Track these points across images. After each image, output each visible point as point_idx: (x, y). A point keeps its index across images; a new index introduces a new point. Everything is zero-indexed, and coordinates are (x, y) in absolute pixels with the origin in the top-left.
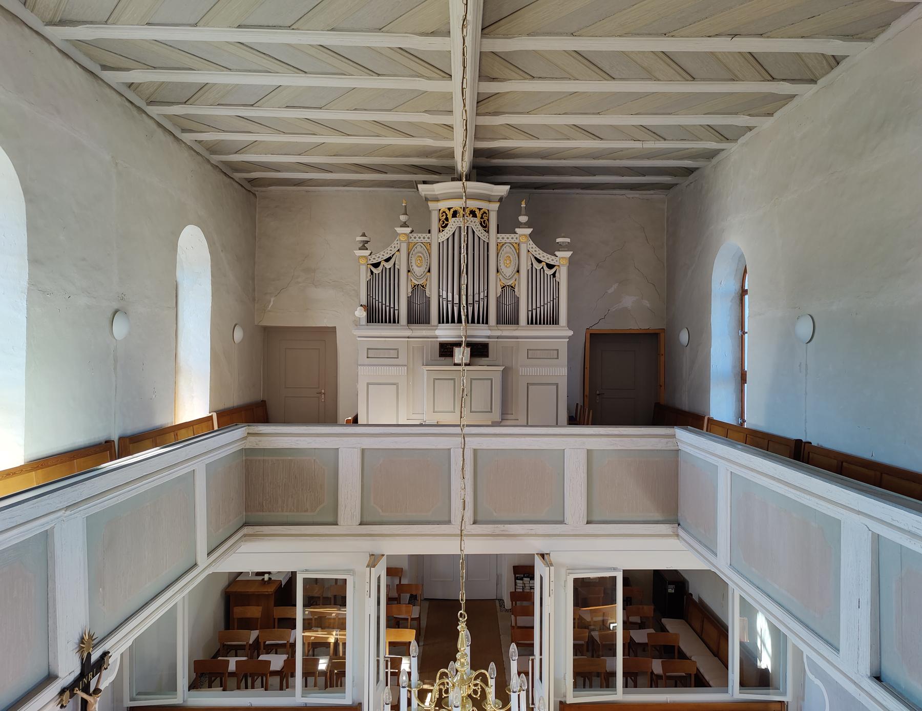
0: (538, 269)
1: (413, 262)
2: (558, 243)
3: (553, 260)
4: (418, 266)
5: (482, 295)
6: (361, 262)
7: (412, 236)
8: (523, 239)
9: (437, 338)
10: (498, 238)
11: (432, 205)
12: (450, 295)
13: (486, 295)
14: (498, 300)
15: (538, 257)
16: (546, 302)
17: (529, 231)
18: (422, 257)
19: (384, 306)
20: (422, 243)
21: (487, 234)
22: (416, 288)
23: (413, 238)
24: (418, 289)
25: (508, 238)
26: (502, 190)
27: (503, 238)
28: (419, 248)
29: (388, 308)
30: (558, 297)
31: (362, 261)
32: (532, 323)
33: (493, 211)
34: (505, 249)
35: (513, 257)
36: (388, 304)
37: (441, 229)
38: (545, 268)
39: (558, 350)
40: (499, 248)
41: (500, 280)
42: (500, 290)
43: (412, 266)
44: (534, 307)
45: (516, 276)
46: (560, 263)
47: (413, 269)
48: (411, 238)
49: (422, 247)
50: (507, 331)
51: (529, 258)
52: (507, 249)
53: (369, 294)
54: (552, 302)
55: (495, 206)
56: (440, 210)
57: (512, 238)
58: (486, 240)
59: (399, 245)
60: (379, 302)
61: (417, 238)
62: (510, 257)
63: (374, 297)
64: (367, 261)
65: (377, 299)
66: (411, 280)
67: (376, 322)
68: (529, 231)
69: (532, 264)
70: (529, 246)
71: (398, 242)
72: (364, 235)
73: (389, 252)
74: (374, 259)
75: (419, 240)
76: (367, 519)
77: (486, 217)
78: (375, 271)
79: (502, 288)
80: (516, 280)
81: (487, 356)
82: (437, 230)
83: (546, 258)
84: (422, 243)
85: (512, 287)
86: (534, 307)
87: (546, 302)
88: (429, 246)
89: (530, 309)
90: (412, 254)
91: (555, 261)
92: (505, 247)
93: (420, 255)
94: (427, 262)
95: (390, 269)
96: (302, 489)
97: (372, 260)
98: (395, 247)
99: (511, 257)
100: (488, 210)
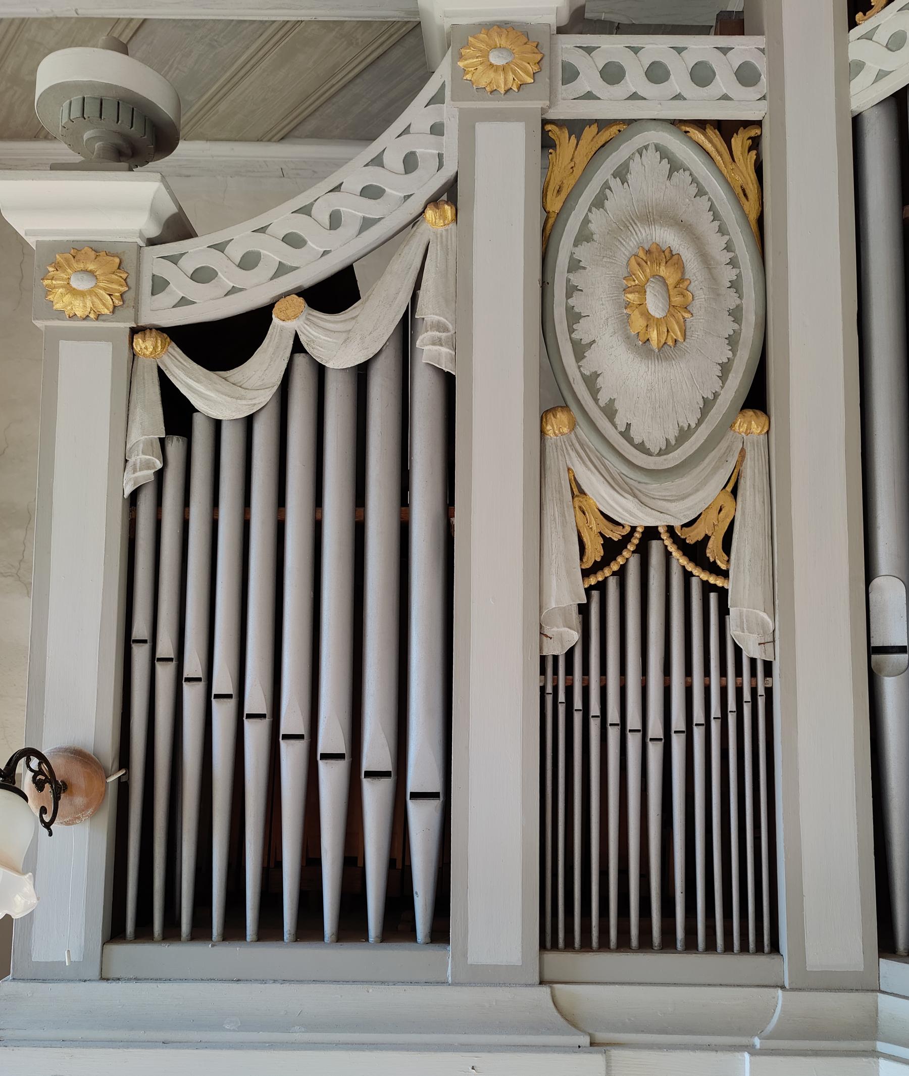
6: (61, 301)
7: (579, 60)
18: (688, 255)
22: (621, 574)
23: (591, 79)
43: (580, 350)
47: (591, 381)
48: (570, 74)
49: (675, 166)
53: (141, 629)
59: (450, 143)
60: (240, 716)
61: (635, 80)
63: (193, 665)
65: (223, 682)
66: (578, 491)
71: (448, 113)
74: (202, 275)
88: (746, 163)
90: (584, 236)
94: (736, 314)
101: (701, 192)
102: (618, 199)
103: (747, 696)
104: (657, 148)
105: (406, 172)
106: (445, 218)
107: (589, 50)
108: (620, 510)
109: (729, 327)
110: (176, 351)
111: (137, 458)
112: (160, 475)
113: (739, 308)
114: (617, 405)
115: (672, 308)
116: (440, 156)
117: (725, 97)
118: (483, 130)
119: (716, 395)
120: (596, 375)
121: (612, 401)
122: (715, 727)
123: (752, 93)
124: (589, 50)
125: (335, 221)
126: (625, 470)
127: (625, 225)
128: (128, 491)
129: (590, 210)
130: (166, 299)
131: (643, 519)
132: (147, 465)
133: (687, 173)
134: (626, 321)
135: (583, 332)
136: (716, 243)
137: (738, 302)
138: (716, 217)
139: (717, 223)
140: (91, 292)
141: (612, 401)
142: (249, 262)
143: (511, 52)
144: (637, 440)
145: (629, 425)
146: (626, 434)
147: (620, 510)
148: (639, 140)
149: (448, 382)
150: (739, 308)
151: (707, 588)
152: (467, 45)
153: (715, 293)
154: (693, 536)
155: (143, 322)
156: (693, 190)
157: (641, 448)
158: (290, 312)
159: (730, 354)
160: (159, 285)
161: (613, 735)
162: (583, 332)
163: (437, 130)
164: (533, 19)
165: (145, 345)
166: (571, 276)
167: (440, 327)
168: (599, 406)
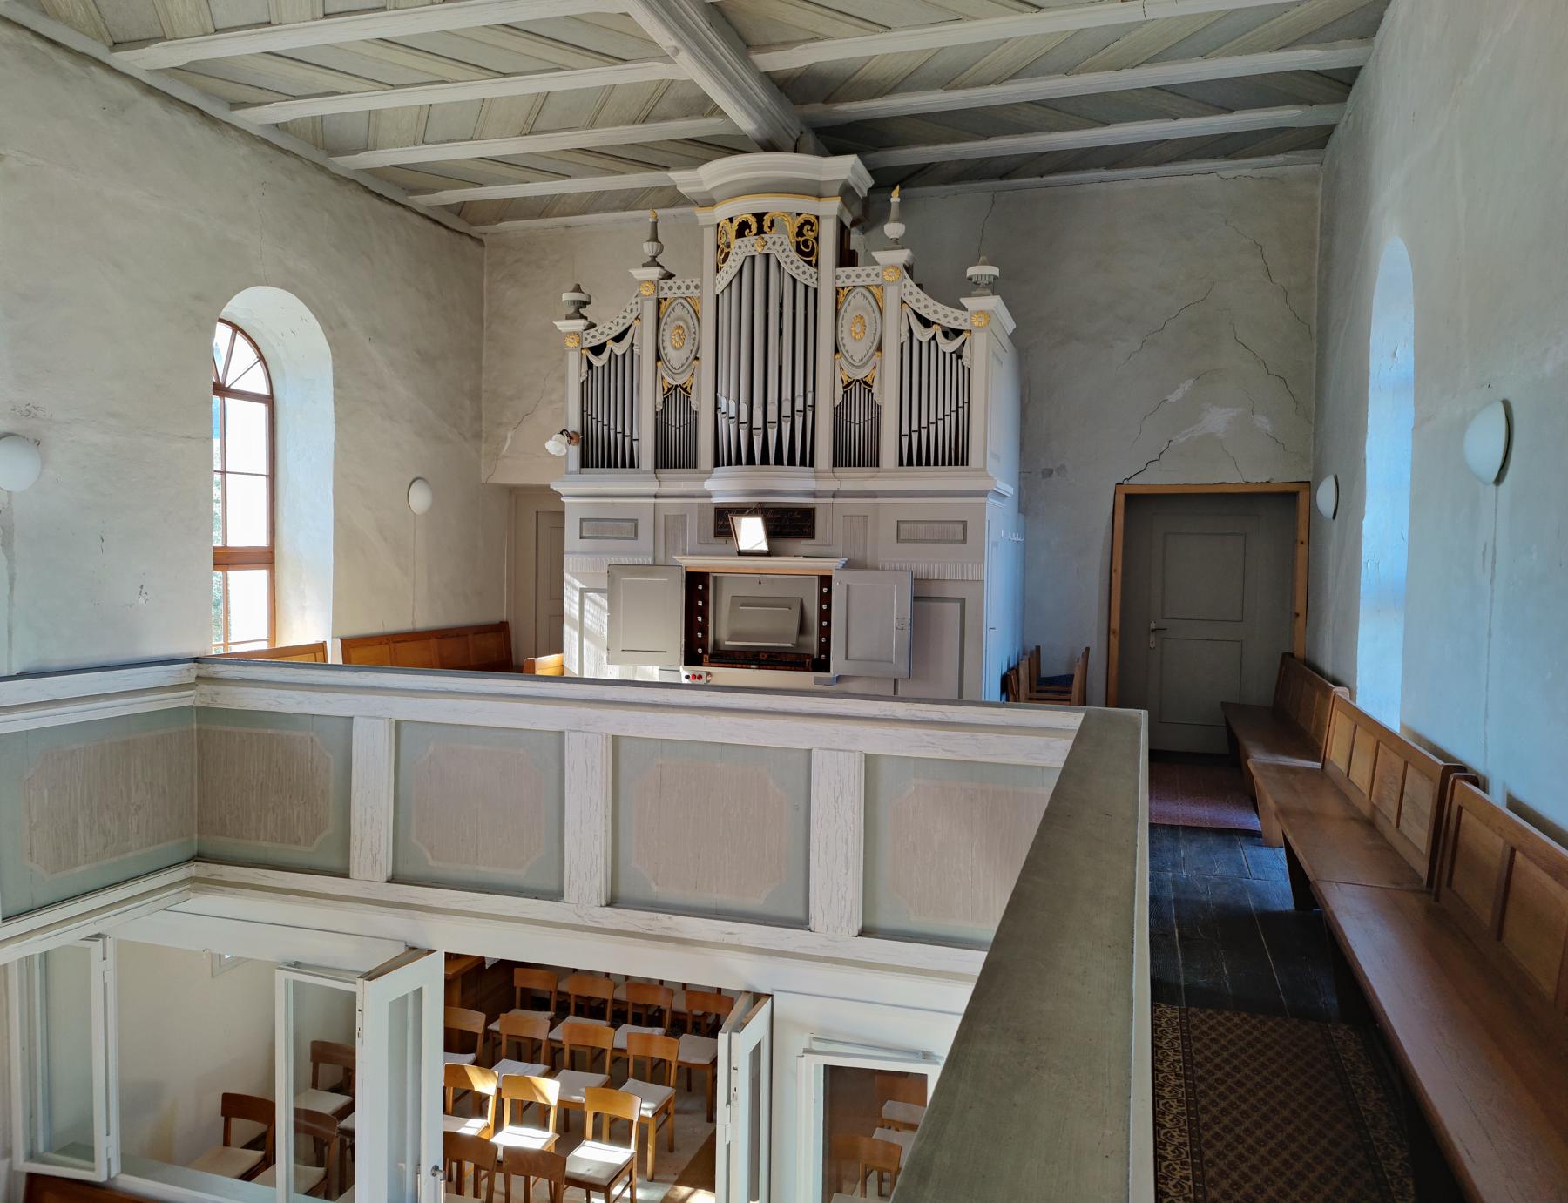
0: (925, 340)
1: (667, 338)
2: (970, 279)
3: (956, 319)
4: (675, 348)
6: (568, 344)
8: (890, 276)
9: (711, 497)
10: (837, 277)
12: (744, 408)
13: (809, 402)
14: (836, 411)
15: (923, 313)
16: (940, 415)
17: (902, 256)
18: (685, 327)
19: (612, 432)
20: (685, 299)
21: (812, 270)
22: (672, 394)
23: (666, 290)
24: (675, 395)
26: (846, 168)
27: (848, 277)
28: (679, 311)
29: (619, 436)
30: (969, 403)
31: (571, 343)
32: (910, 463)
33: (826, 217)
35: (869, 315)
36: (619, 429)
38: (940, 337)
39: (964, 523)
40: (841, 298)
41: (842, 370)
42: (839, 391)
44: (915, 427)
46: (971, 323)
47: (666, 355)
48: (662, 289)
49: (684, 307)
50: (855, 479)
51: (904, 316)
52: (856, 304)
53: (585, 409)
54: (954, 415)
55: (829, 210)
56: (718, 225)
57: (868, 275)
58: (811, 283)
61: (675, 290)
62: (862, 317)
64: (580, 343)
66: (663, 378)
67: (597, 466)
68: (902, 256)
70: (903, 290)
71: (639, 299)
72: (578, 289)
73: (621, 321)
74: (594, 337)
75: (679, 294)
76: (407, 869)
77: (810, 233)
78: (598, 362)
79: (844, 388)
80: (875, 368)
81: (810, 535)
82: (713, 267)
83: (940, 315)
85: (866, 383)
86: (915, 427)
87: (940, 415)
89: (905, 431)
90: (666, 324)
91: (961, 321)
92: (854, 297)
93: (681, 324)
94: (694, 339)
95: (624, 355)
96: (290, 797)
97: (590, 339)
98: (632, 310)
99: (866, 317)
100: (817, 217)
111: (583, 374)
118: (645, 302)
125: (618, 323)
131: (675, 383)
142: (602, 333)
148: (677, 301)
149: (639, 356)
151: (688, 397)
153: (690, 335)
154: (684, 386)
163: (637, 303)
165: (583, 352)
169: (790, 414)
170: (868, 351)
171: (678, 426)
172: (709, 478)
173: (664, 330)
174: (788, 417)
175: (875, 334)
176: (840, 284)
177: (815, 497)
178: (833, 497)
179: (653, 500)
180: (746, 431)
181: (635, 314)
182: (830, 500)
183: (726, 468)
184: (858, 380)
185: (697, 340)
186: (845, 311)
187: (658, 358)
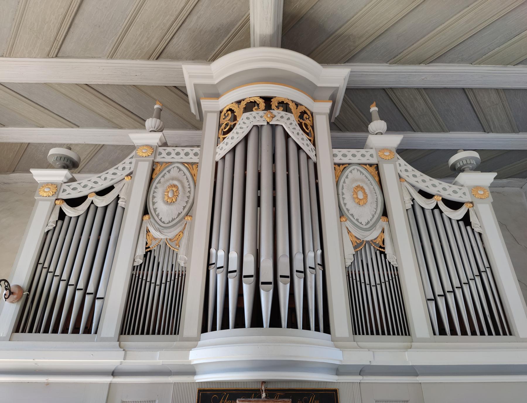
4: (167, 203)
5: (310, 255)
7: (163, 152)
10: (335, 155)
11: (206, 104)
13: (319, 261)
25: (354, 156)
27: (344, 156)
28: (174, 172)
30: (490, 267)
34: (350, 174)
35: (367, 184)
37: (222, 137)
41: (349, 232)
42: (350, 251)
43: (154, 203)
45: (383, 223)
47: (155, 210)
48: (160, 154)
49: (180, 170)
53: (41, 261)
56: (221, 112)
59: (133, 166)
62: (362, 188)
64: (56, 193)
66: (148, 231)
69: (413, 200)
70: (399, 168)
71: (134, 160)
74: (74, 189)
75: (177, 159)
79: (355, 248)
80: (383, 231)
84: (183, 163)
92: (351, 172)
94: (189, 197)
99: (365, 187)
101: (185, 175)
102: (168, 176)
103: (180, 275)
104: (177, 167)
105: (122, 170)
106: (129, 179)
107: (165, 150)
108: (156, 235)
109: (187, 199)
110: (65, 204)
111: (49, 224)
112: (55, 228)
113: (189, 196)
114: (160, 214)
115: (174, 195)
116: (130, 168)
117: (191, 158)
118: (139, 163)
119: (181, 212)
120: (156, 208)
121: (159, 213)
122: (172, 282)
123: (197, 157)
124: (165, 150)
126: (159, 227)
127: (168, 180)
128: (46, 231)
129: (161, 178)
130: (65, 193)
132: (52, 226)
133: (183, 171)
134: (164, 198)
135: (155, 200)
136: (186, 184)
137: (189, 195)
138: (187, 179)
139: (187, 180)
140: (49, 191)
141: (159, 213)
142: (85, 186)
143: (147, 150)
144: (163, 221)
145: (161, 218)
146: (160, 220)
147: (156, 235)
148: (173, 166)
150: (189, 196)
152: (139, 148)
153: (184, 193)
155: (59, 198)
156: (183, 174)
157: (164, 223)
158: (92, 196)
159: (186, 205)
160: (64, 191)
161: (148, 284)
162: (155, 200)
164: (153, 144)
165: (58, 202)
166: (155, 190)
167: (123, 199)
168: (156, 215)
169: (288, 274)
170: (373, 216)
171: (158, 282)
172: (195, 346)
173: (156, 188)
174: (270, 283)
175: (377, 202)
176: (337, 160)
177: (337, 374)
178: (360, 375)
179: (109, 379)
180: (253, 285)
181: (127, 172)
182: (357, 379)
183: (219, 332)
184: (367, 242)
185: (192, 198)
186: (344, 182)
187: (146, 212)
